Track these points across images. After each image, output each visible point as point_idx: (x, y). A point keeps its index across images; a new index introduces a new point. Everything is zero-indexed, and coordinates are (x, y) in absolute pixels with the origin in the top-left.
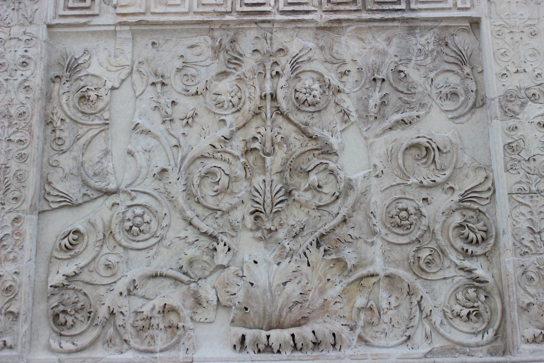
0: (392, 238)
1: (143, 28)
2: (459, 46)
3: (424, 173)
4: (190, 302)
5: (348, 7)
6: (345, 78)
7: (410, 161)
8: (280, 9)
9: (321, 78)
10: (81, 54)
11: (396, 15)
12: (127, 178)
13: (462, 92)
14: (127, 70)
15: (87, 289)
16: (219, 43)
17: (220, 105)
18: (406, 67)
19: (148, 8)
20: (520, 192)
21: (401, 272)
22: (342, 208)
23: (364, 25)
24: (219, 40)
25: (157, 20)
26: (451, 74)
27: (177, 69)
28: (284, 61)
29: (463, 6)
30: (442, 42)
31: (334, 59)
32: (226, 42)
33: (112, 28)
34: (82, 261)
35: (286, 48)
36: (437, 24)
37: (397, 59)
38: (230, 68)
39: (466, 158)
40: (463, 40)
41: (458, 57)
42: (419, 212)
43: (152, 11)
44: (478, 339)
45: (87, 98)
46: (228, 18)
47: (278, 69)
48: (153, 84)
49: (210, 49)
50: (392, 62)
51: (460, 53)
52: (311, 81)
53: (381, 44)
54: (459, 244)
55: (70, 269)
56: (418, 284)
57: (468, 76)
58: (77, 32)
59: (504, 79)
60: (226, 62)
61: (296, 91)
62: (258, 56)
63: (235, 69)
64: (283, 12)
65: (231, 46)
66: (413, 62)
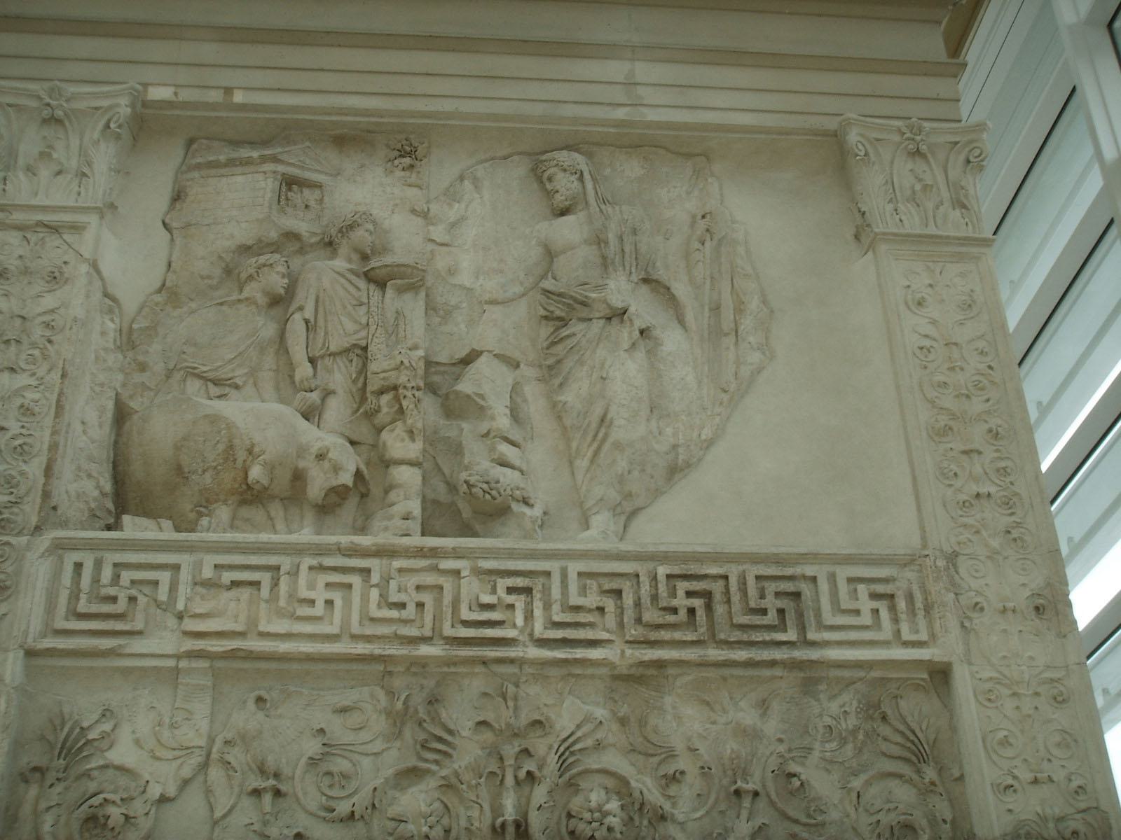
1: (237, 664)
2: (909, 719)
5: (678, 635)
6: (673, 790)
8: (537, 634)
9: (622, 787)
10: (95, 717)
11: (777, 654)
13: (924, 822)
14: (196, 759)
16: (404, 703)
18: (803, 764)
19: (253, 622)
23: (711, 673)
24: (403, 698)
25: (272, 649)
26: (897, 781)
27: (311, 758)
29: (914, 637)
30: (873, 711)
31: (649, 745)
32: (418, 700)
33: (171, 663)
35: (548, 719)
36: (862, 674)
37: (781, 748)
38: (426, 761)
40: (916, 708)
41: (909, 744)
43: (261, 628)
45: (102, 820)
46: (425, 650)
47: (529, 765)
48: (257, 793)
49: (383, 717)
50: (772, 754)
51: (912, 737)
52: (603, 793)
53: (749, 717)
57: (932, 788)
58: (91, 668)
59: (1010, 798)
60: (418, 747)
61: (570, 816)
62: (488, 736)
63: (437, 762)
64: (542, 643)
65: (429, 712)
66: (816, 754)
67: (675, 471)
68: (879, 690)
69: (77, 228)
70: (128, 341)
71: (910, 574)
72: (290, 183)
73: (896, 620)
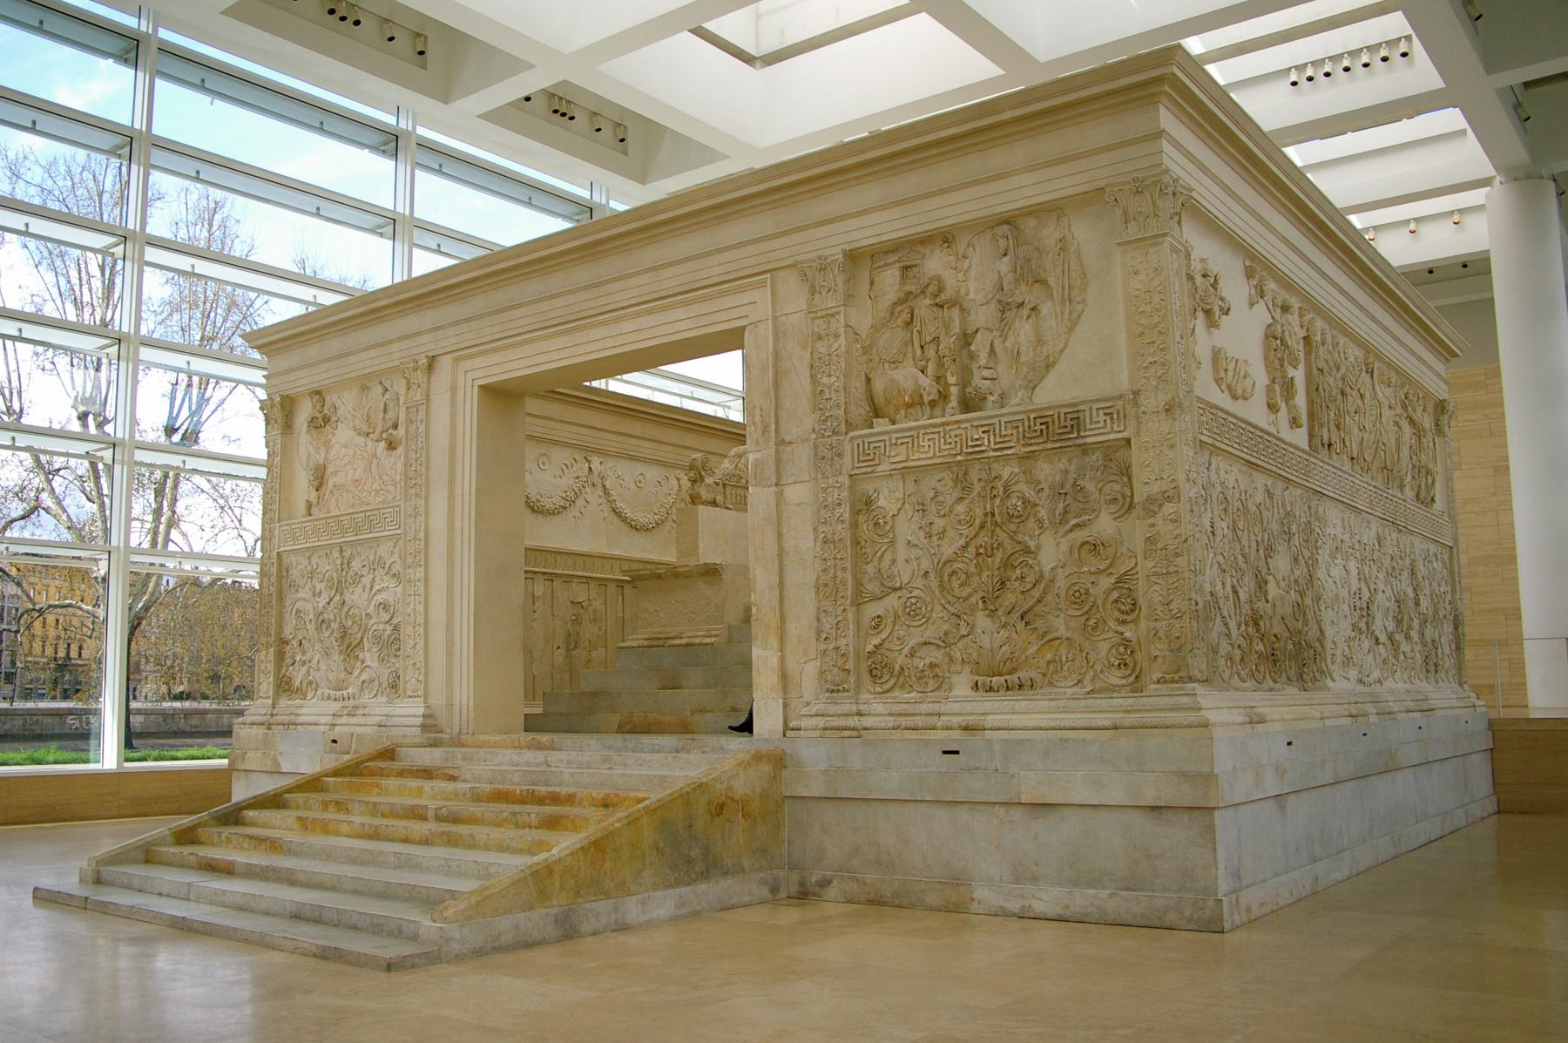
7: (1084, 553)
12: (906, 578)
17: (959, 522)
22: (1036, 593)
28: (999, 485)
39: (1124, 550)
42: (1087, 592)
54: (1116, 613)
55: (877, 641)
56: (1087, 644)
67: (1049, 366)
68: (1109, 449)
70: (865, 351)
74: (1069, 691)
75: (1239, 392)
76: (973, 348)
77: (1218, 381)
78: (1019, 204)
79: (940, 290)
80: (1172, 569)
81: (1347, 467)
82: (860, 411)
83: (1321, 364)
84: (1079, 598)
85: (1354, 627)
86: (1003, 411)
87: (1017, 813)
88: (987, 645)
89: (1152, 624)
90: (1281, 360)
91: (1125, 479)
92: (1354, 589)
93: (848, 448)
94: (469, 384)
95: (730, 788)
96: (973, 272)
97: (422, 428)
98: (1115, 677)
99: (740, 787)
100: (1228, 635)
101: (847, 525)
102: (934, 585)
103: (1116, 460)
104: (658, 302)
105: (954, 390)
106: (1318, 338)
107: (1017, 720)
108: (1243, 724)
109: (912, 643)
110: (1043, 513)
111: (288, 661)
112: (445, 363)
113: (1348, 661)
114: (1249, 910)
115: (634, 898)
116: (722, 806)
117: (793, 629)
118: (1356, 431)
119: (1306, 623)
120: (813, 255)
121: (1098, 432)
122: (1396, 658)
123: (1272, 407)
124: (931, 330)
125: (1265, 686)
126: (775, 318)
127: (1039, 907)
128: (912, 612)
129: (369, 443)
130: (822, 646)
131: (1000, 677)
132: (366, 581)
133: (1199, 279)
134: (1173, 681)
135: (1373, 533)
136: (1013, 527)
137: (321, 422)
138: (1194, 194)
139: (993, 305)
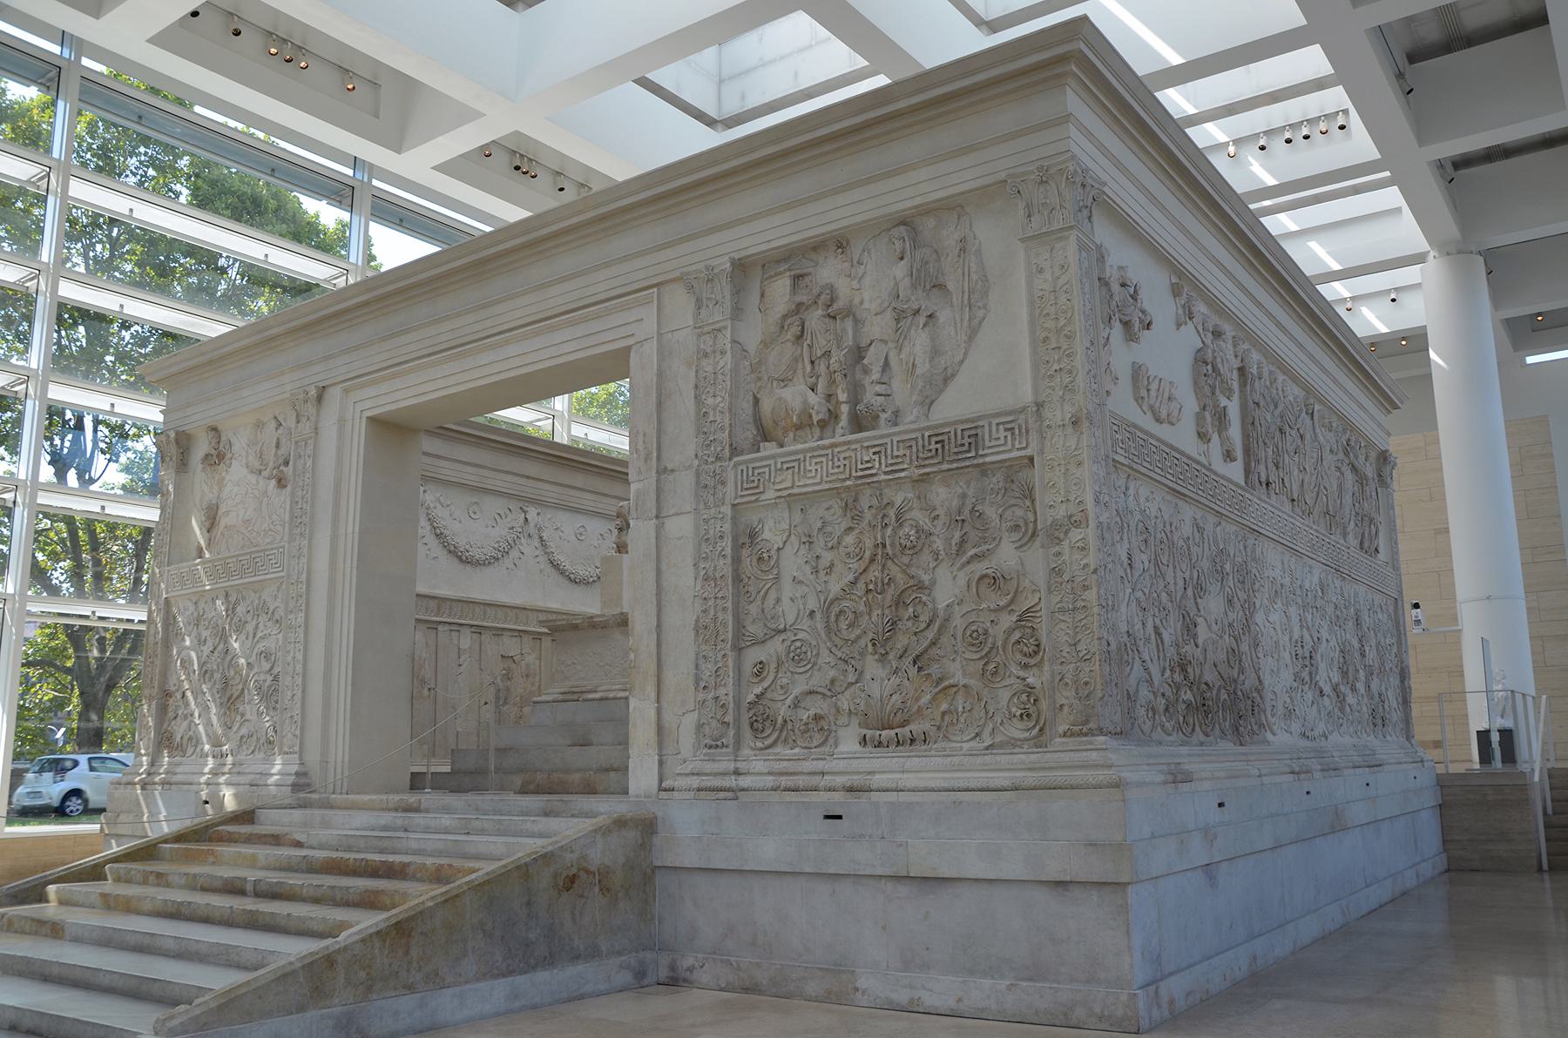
0: (968, 655)
3: (994, 599)
4: (833, 710)
12: (790, 619)
15: (770, 704)
20: (1061, 610)
21: (972, 682)
28: (892, 513)
34: (766, 685)
39: (1027, 583)
42: (986, 633)
44: (1026, 735)
46: (848, 483)
54: (1019, 656)
55: (758, 690)
64: (886, 473)
67: (947, 380)
69: (725, 328)
71: (1022, 416)
72: (797, 278)
73: (1014, 439)
74: (966, 746)
75: (1164, 415)
76: (865, 361)
77: (1139, 400)
78: (917, 201)
79: (832, 301)
80: (1080, 604)
81: (1287, 507)
82: (751, 433)
83: (1257, 397)
84: (977, 639)
85: (1297, 677)
86: (896, 429)
87: (904, 890)
88: (876, 693)
89: (1057, 668)
90: (1213, 388)
91: (1028, 503)
92: (1296, 636)
93: (730, 475)
94: (358, 415)
95: (584, 857)
96: (867, 280)
97: (309, 463)
98: (1016, 730)
99: (597, 856)
100: (1150, 681)
101: (729, 560)
102: (820, 626)
103: (1016, 478)
104: (545, 322)
105: (845, 409)
106: (1254, 371)
107: (909, 780)
108: (1165, 783)
109: (797, 691)
110: (939, 544)
111: (171, 715)
112: (334, 394)
113: (1289, 713)
114: (1172, 1002)
115: (450, 991)
116: (572, 879)
117: (670, 678)
118: (1296, 472)
119: (1242, 671)
120: (701, 266)
121: (999, 448)
122: (1342, 710)
123: (1202, 436)
124: (821, 343)
125: (1194, 739)
126: (660, 335)
127: (930, 1000)
128: (798, 657)
129: (262, 482)
130: (701, 696)
131: (890, 730)
132: (250, 627)
133: (1116, 287)
134: (1081, 734)
135: (1316, 580)
136: (906, 560)
137: (217, 458)
138: (1106, 189)
139: (889, 314)
